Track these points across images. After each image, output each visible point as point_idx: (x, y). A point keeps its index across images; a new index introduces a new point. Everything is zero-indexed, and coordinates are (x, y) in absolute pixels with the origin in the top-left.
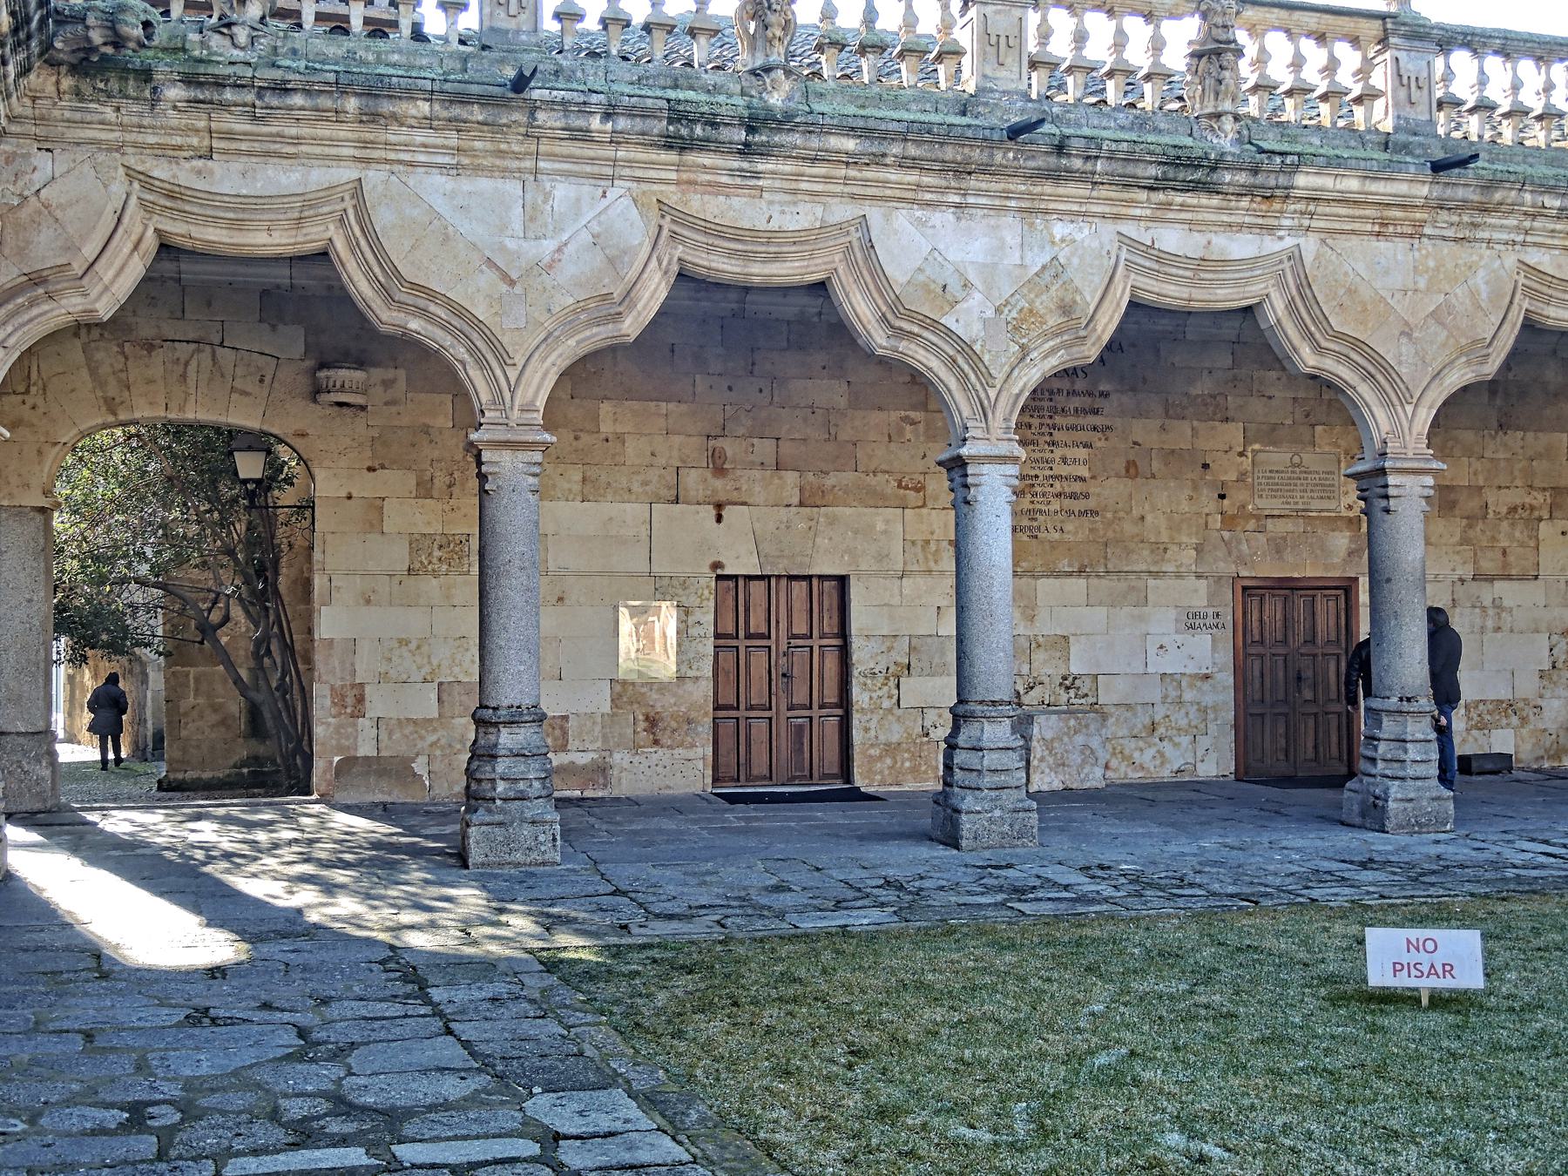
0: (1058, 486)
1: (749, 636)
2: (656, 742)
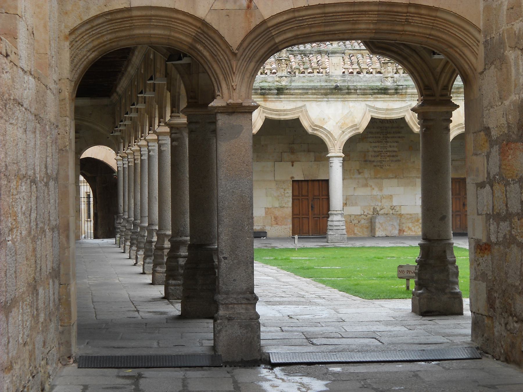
0: (388, 154)
1: (302, 196)
2: (277, 224)
